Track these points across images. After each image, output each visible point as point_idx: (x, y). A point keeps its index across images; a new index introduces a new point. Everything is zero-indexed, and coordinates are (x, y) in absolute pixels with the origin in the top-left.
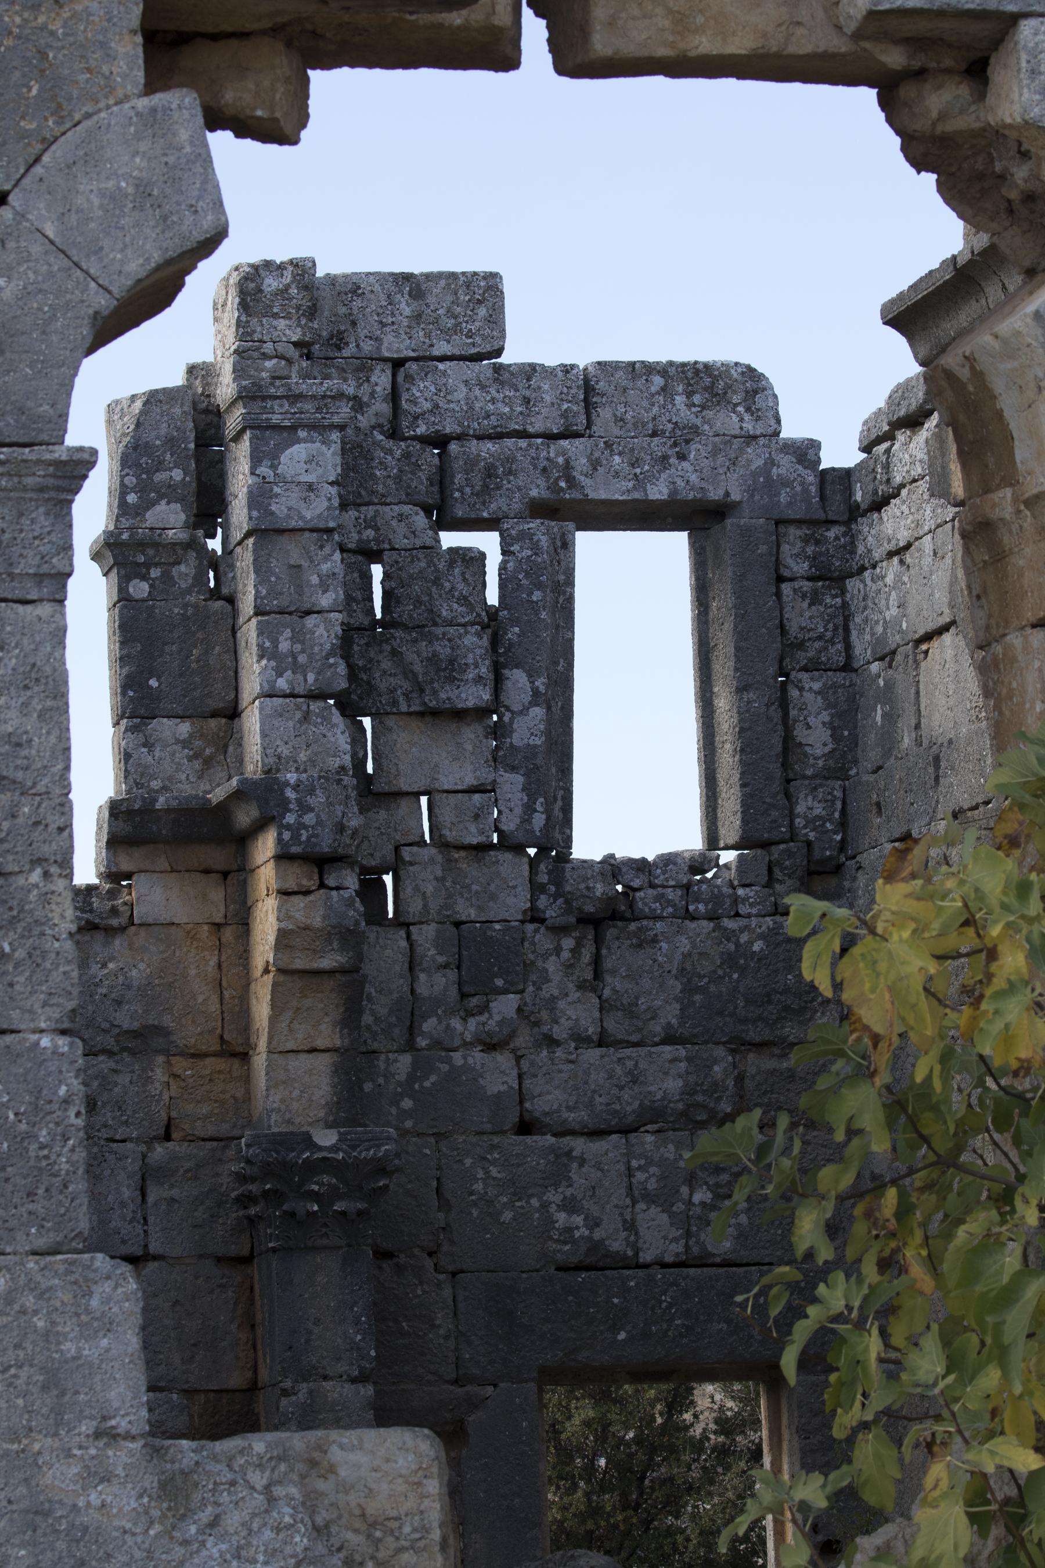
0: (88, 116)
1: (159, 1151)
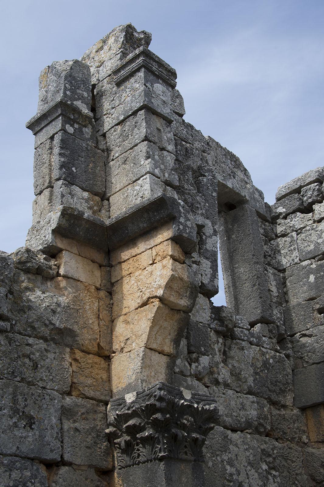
1: (68, 399)
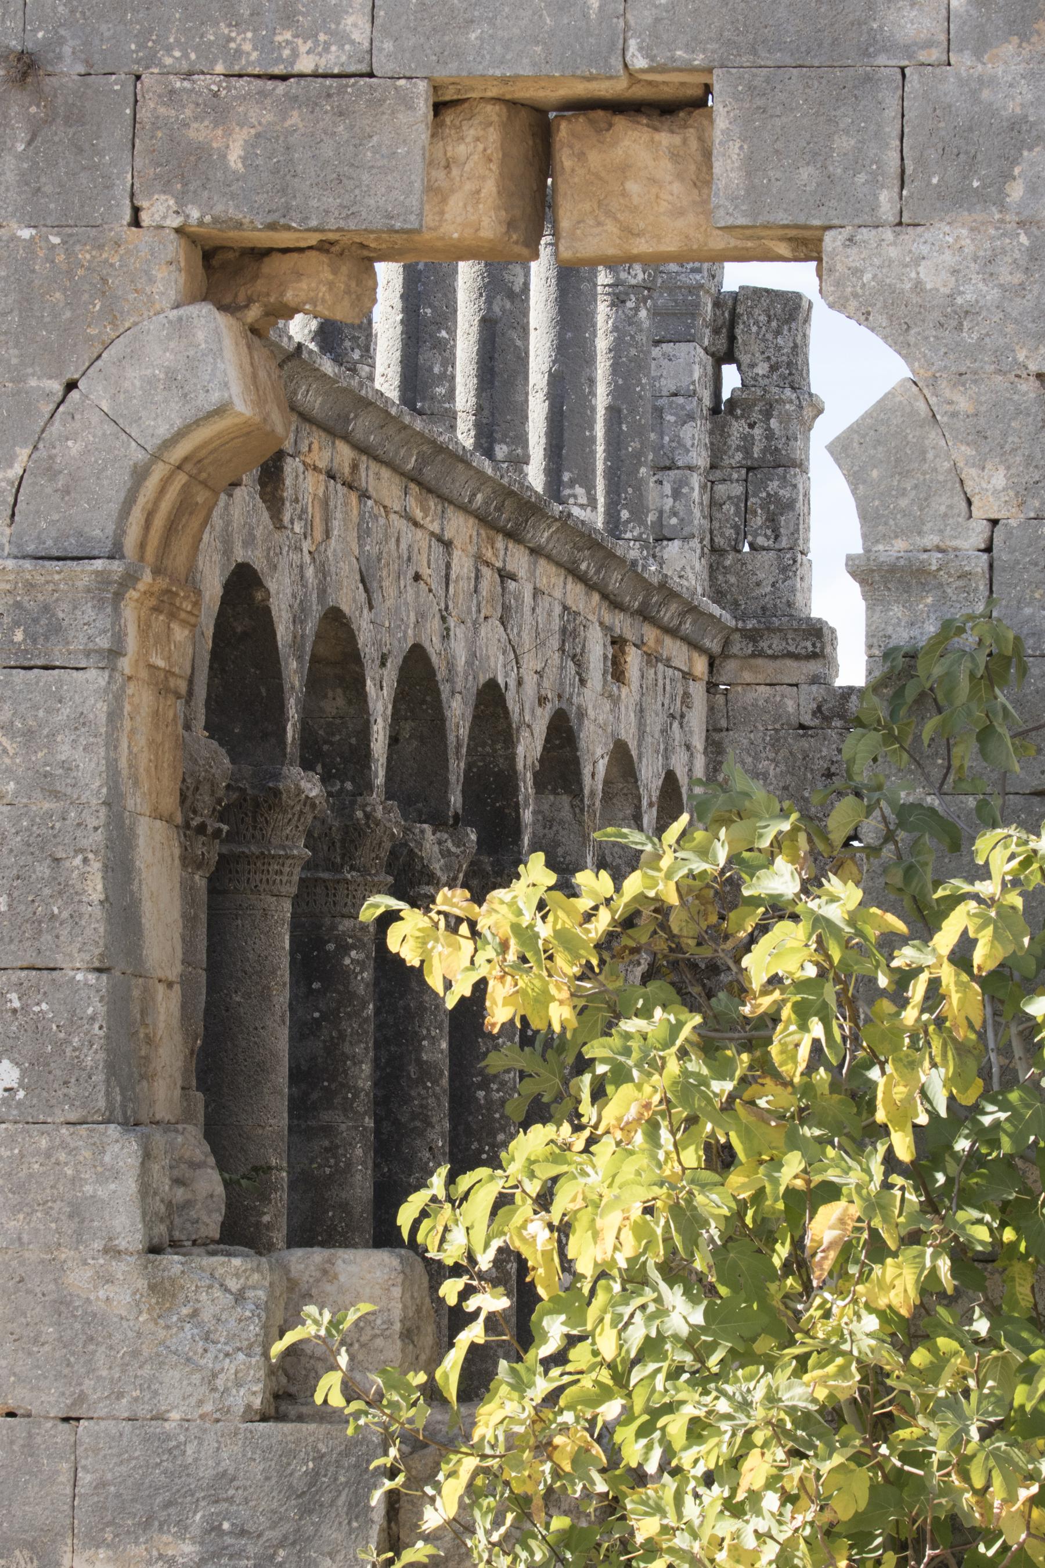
0: (136, 324)
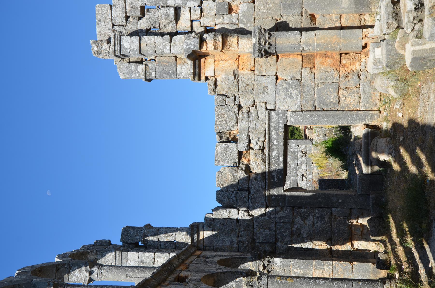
1: (256, 72)
